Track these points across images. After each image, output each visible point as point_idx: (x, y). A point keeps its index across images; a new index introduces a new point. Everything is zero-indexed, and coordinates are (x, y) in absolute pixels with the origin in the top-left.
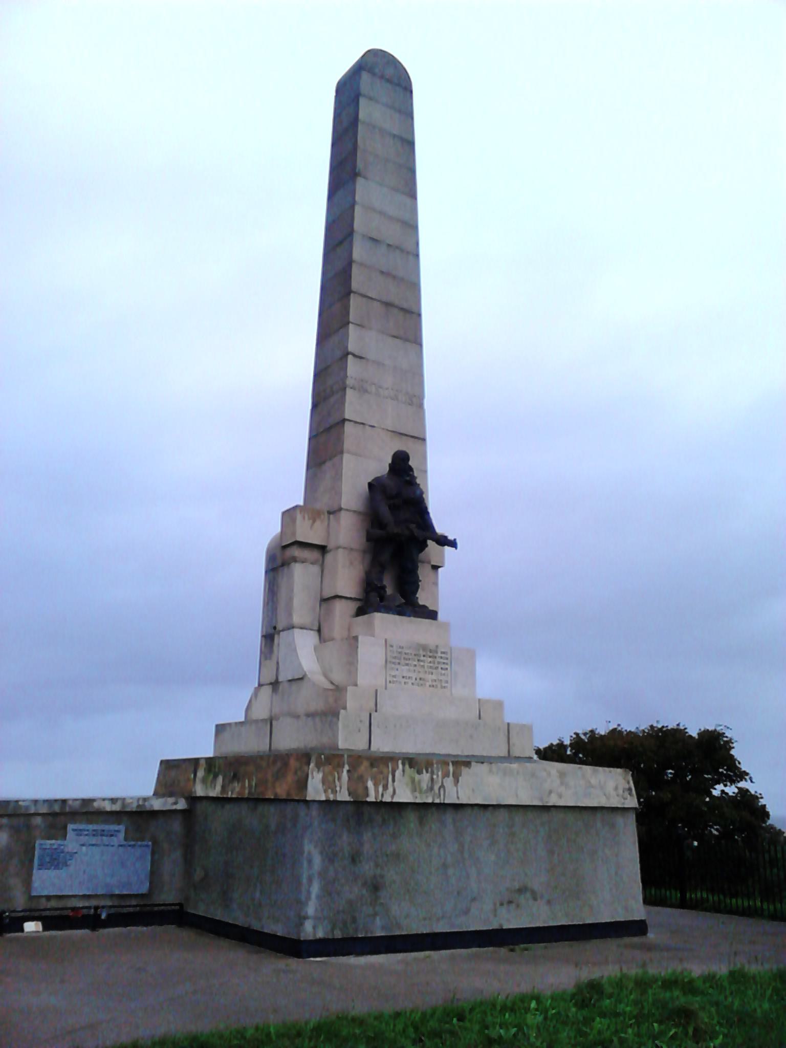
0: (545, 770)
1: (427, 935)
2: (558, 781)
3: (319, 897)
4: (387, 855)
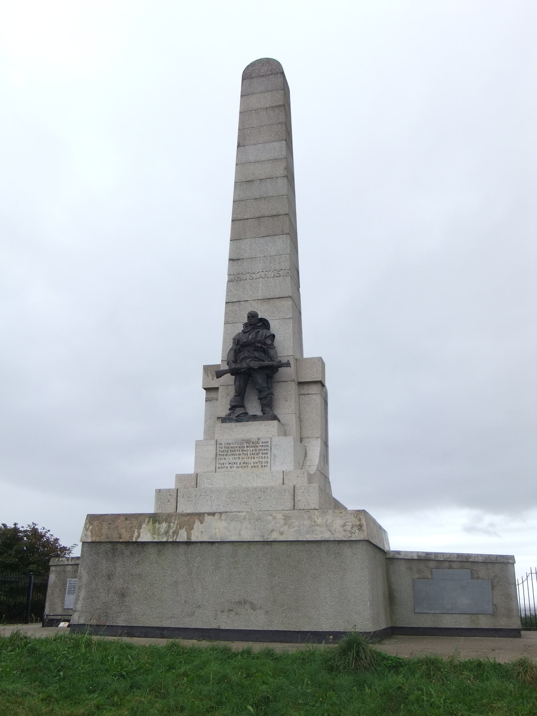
1: (158, 628)
2: (282, 522)
3: (83, 599)
4: (132, 575)
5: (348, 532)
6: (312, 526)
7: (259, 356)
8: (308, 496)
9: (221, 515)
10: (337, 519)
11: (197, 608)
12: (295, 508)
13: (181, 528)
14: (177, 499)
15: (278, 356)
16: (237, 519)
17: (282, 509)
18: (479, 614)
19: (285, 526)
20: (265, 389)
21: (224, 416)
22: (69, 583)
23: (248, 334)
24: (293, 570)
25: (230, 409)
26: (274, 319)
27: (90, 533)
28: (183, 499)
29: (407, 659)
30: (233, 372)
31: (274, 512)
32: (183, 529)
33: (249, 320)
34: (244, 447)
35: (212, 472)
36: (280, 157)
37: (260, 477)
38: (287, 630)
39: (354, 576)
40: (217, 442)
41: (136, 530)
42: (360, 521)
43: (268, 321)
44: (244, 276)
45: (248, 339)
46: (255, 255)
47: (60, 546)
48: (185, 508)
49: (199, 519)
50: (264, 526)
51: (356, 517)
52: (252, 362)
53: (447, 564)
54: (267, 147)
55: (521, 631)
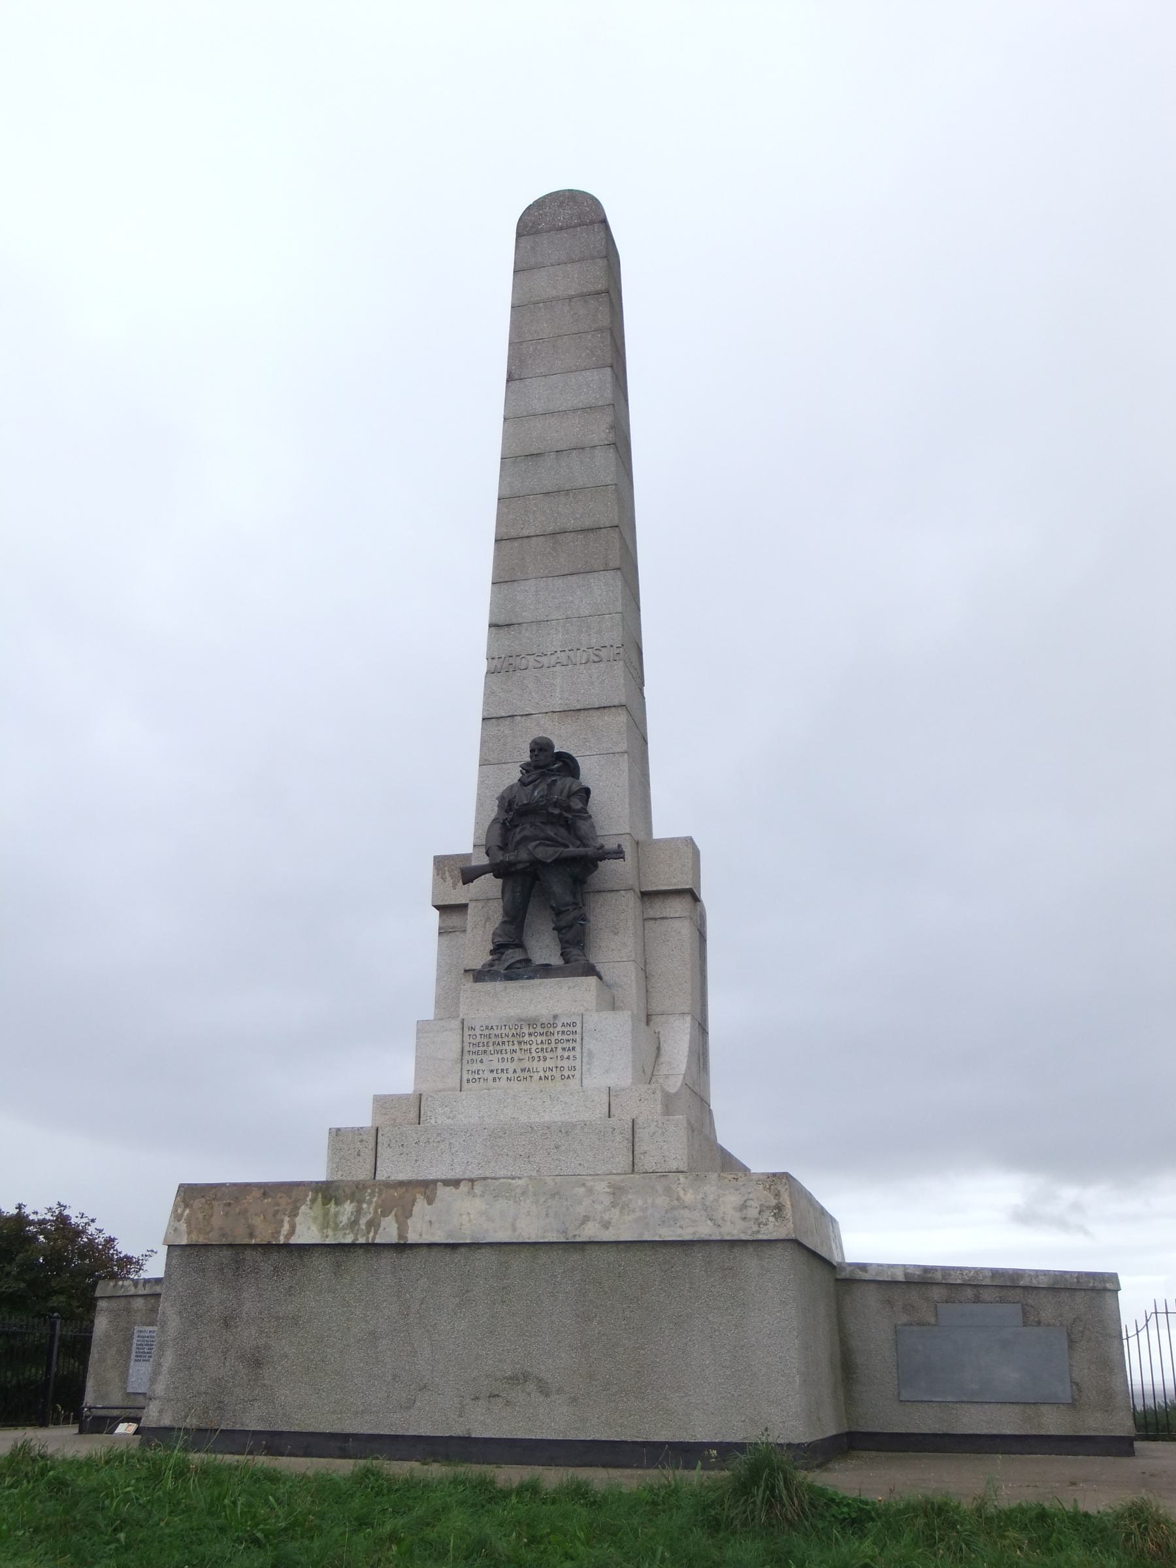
0: (584, 1185)
1: (333, 1436)
2: (607, 1200)
3: (169, 1372)
4: (278, 1318)
5: (752, 1223)
6: (673, 1208)
7: (555, 834)
8: (664, 1141)
9: (473, 1185)
10: (727, 1192)
11: (420, 1390)
12: (636, 1170)
13: (385, 1214)
14: (376, 1151)
15: (598, 834)
16: (508, 1194)
17: (608, 1172)
18: (1041, 1403)
19: (613, 1209)
20: (568, 908)
21: (479, 967)
22: (138, 1337)
23: (530, 787)
24: (631, 1305)
25: (492, 952)
26: (588, 753)
27: (185, 1225)
28: (389, 1150)
29: (882, 1503)
30: (499, 870)
31: (590, 1178)
32: (390, 1216)
33: (534, 758)
34: (524, 1035)
35: (453, 1089)
36: (600, 403)
37: (558, 1101)
38: (618, 1440)
39: (765, 1320)
40: (463, 1023)
41: (287, 1219)
42: (777, 1197)
43: (576, 760)
44: (523, 661)
45: (532, 798)
46: (547, 616)
47: (117, 1255)
48: (393, 1169)
49: (425, 1193)
50: (568, 1209)
51: (770, 1189)
52: (541, 849)
53: (969, 1293)
54: (571, 381)
55: (1135, 1442)
